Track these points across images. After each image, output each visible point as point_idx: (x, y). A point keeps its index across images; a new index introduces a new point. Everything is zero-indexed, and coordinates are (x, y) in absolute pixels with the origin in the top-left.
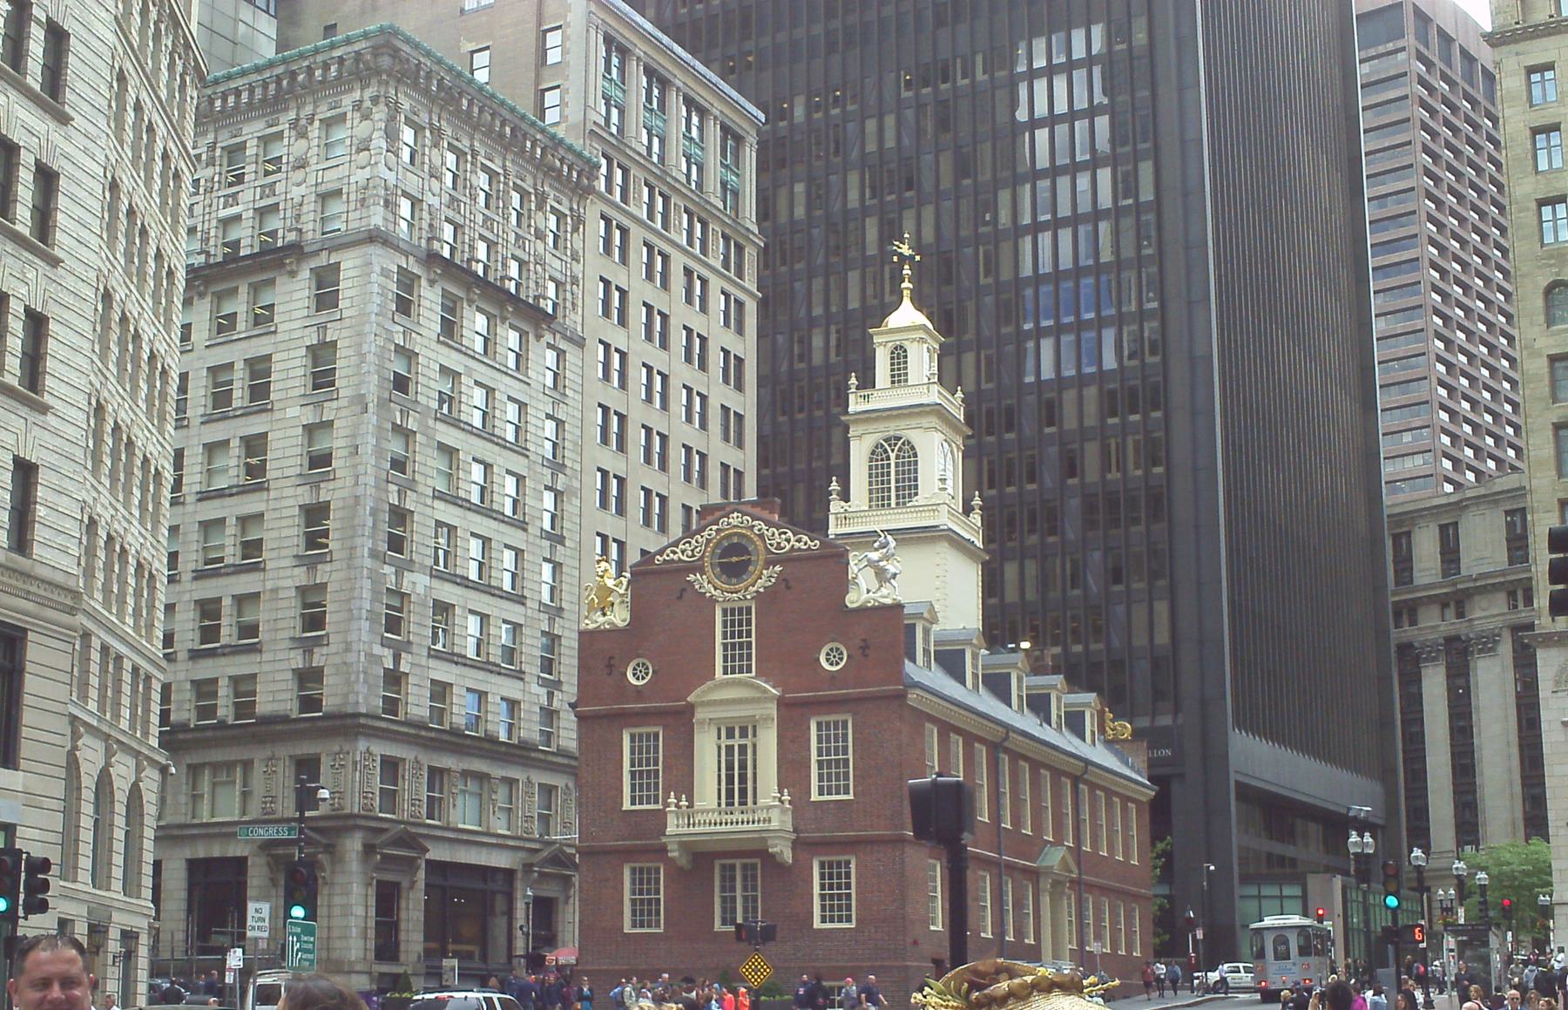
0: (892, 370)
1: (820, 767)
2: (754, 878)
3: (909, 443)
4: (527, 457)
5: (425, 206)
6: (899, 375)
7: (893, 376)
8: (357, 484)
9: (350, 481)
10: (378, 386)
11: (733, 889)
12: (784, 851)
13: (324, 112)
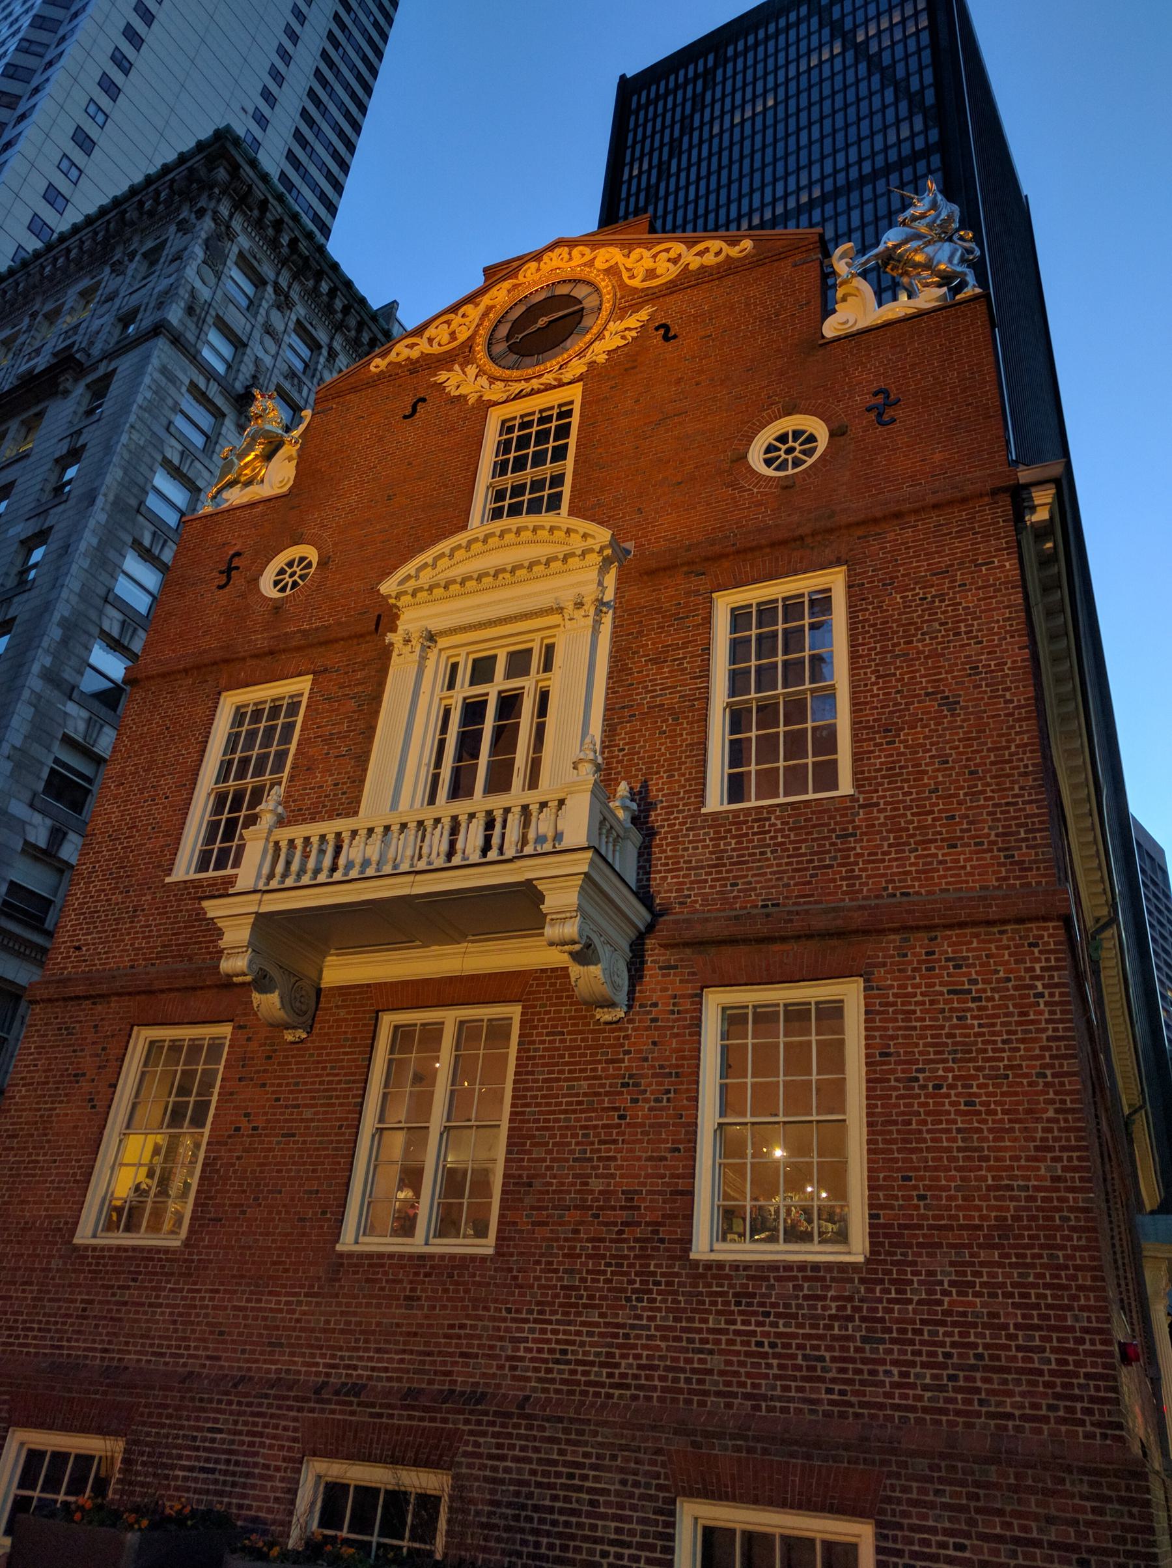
5: (248, 351)
10: (119, 483)
13: (150, 244)
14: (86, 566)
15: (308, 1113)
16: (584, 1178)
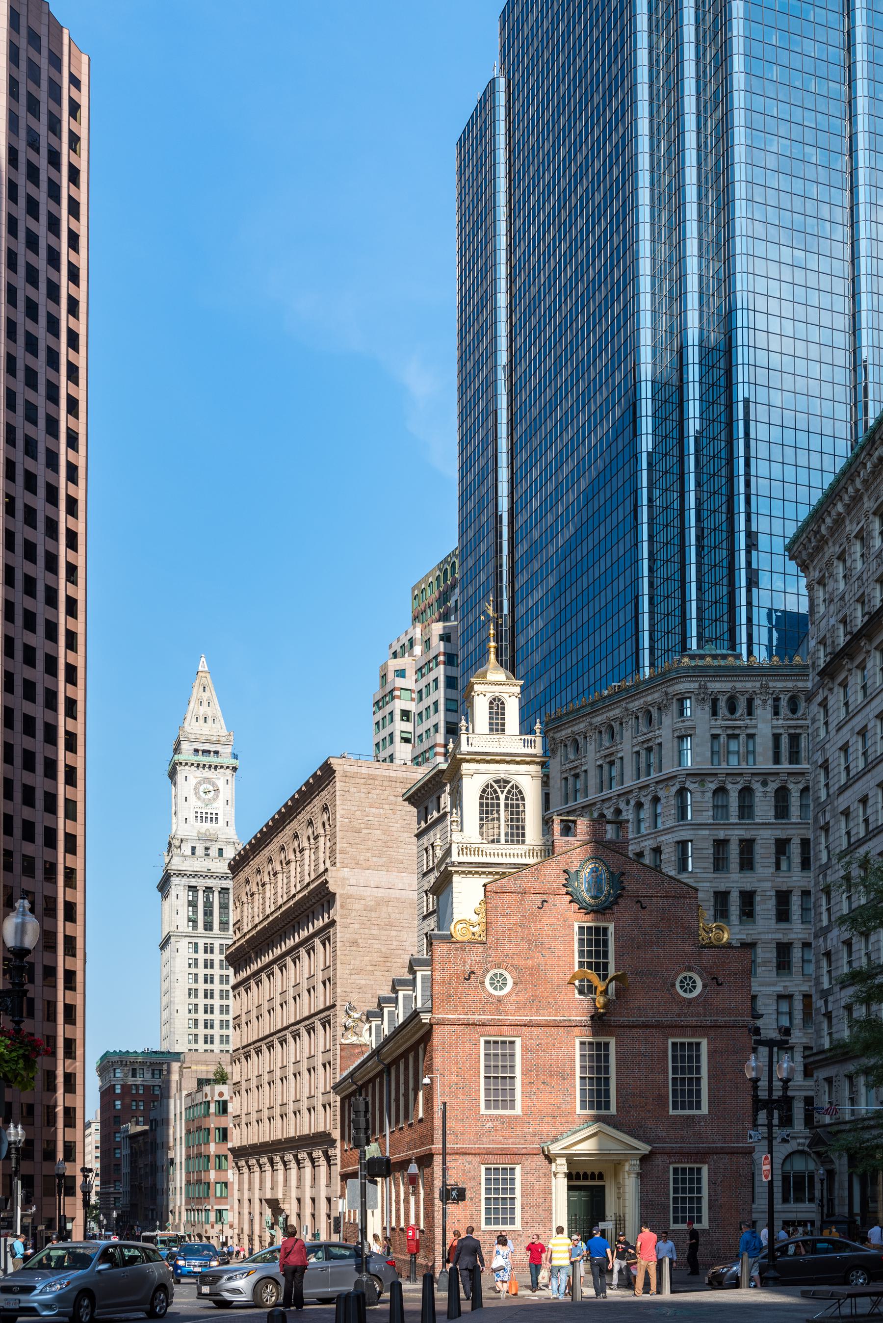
0: (491, 718)
3: (517, 787)
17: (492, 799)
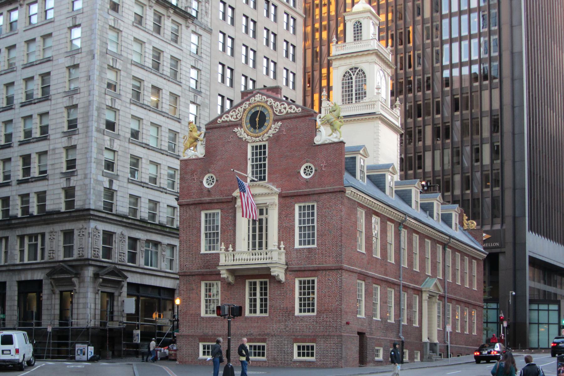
1: (300, 230)
2: (266, 289)
3: (362, 70)
4: (181, 86)
6: (358, 36)
7: (355, 37)
8: (90, 95)
9: (87, 94)
11: (255, 294)
12: (279, 272)
14: (97, 84)
15: (237, 296)
16: (280, 305)
17: (349, 79)
